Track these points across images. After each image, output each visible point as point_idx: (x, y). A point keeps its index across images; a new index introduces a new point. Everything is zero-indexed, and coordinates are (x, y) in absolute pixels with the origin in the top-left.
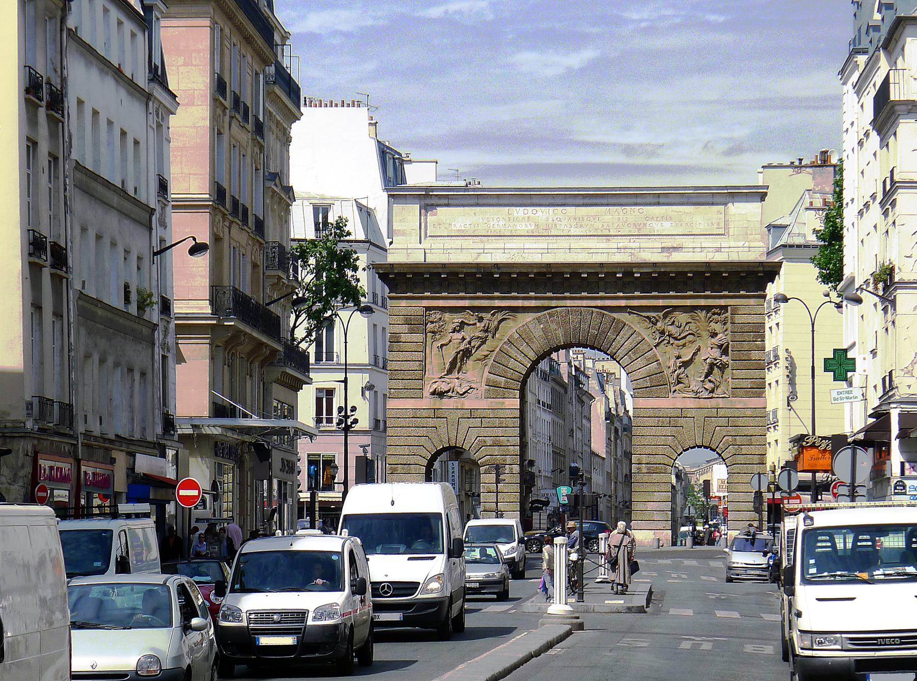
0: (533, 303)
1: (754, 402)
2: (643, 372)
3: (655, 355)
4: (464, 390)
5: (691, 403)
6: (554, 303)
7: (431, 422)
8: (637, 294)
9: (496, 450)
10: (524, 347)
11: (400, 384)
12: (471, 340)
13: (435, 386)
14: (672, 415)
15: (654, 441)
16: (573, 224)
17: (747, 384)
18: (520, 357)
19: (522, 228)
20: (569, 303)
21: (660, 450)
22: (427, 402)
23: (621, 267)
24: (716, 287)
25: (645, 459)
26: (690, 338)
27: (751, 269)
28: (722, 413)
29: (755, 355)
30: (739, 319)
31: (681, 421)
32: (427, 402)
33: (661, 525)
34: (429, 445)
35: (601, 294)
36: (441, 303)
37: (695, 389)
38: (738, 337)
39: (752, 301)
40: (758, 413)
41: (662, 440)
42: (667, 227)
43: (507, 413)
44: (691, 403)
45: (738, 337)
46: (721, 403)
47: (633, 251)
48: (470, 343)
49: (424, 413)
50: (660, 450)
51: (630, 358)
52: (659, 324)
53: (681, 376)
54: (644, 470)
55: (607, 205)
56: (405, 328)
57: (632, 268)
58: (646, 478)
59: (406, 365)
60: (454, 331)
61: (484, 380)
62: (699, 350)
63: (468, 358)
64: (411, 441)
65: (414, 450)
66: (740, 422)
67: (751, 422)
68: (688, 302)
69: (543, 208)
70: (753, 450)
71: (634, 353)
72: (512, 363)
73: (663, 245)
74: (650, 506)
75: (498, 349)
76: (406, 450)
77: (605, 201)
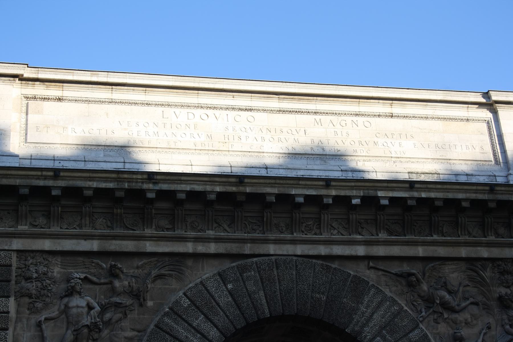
0: (213, 248)
8: (383, 236)
10: (199, 321)
12: (104, 309)
20: (272, 249)
24: (502, 230)
26: (475, 309)
35: (324, 236)
36: (47, 245)
52: (425, 287)
60: (71, 292)
68: (463, 252)
69: (217, 112)
73: (410, 170)
75: (152, 326)
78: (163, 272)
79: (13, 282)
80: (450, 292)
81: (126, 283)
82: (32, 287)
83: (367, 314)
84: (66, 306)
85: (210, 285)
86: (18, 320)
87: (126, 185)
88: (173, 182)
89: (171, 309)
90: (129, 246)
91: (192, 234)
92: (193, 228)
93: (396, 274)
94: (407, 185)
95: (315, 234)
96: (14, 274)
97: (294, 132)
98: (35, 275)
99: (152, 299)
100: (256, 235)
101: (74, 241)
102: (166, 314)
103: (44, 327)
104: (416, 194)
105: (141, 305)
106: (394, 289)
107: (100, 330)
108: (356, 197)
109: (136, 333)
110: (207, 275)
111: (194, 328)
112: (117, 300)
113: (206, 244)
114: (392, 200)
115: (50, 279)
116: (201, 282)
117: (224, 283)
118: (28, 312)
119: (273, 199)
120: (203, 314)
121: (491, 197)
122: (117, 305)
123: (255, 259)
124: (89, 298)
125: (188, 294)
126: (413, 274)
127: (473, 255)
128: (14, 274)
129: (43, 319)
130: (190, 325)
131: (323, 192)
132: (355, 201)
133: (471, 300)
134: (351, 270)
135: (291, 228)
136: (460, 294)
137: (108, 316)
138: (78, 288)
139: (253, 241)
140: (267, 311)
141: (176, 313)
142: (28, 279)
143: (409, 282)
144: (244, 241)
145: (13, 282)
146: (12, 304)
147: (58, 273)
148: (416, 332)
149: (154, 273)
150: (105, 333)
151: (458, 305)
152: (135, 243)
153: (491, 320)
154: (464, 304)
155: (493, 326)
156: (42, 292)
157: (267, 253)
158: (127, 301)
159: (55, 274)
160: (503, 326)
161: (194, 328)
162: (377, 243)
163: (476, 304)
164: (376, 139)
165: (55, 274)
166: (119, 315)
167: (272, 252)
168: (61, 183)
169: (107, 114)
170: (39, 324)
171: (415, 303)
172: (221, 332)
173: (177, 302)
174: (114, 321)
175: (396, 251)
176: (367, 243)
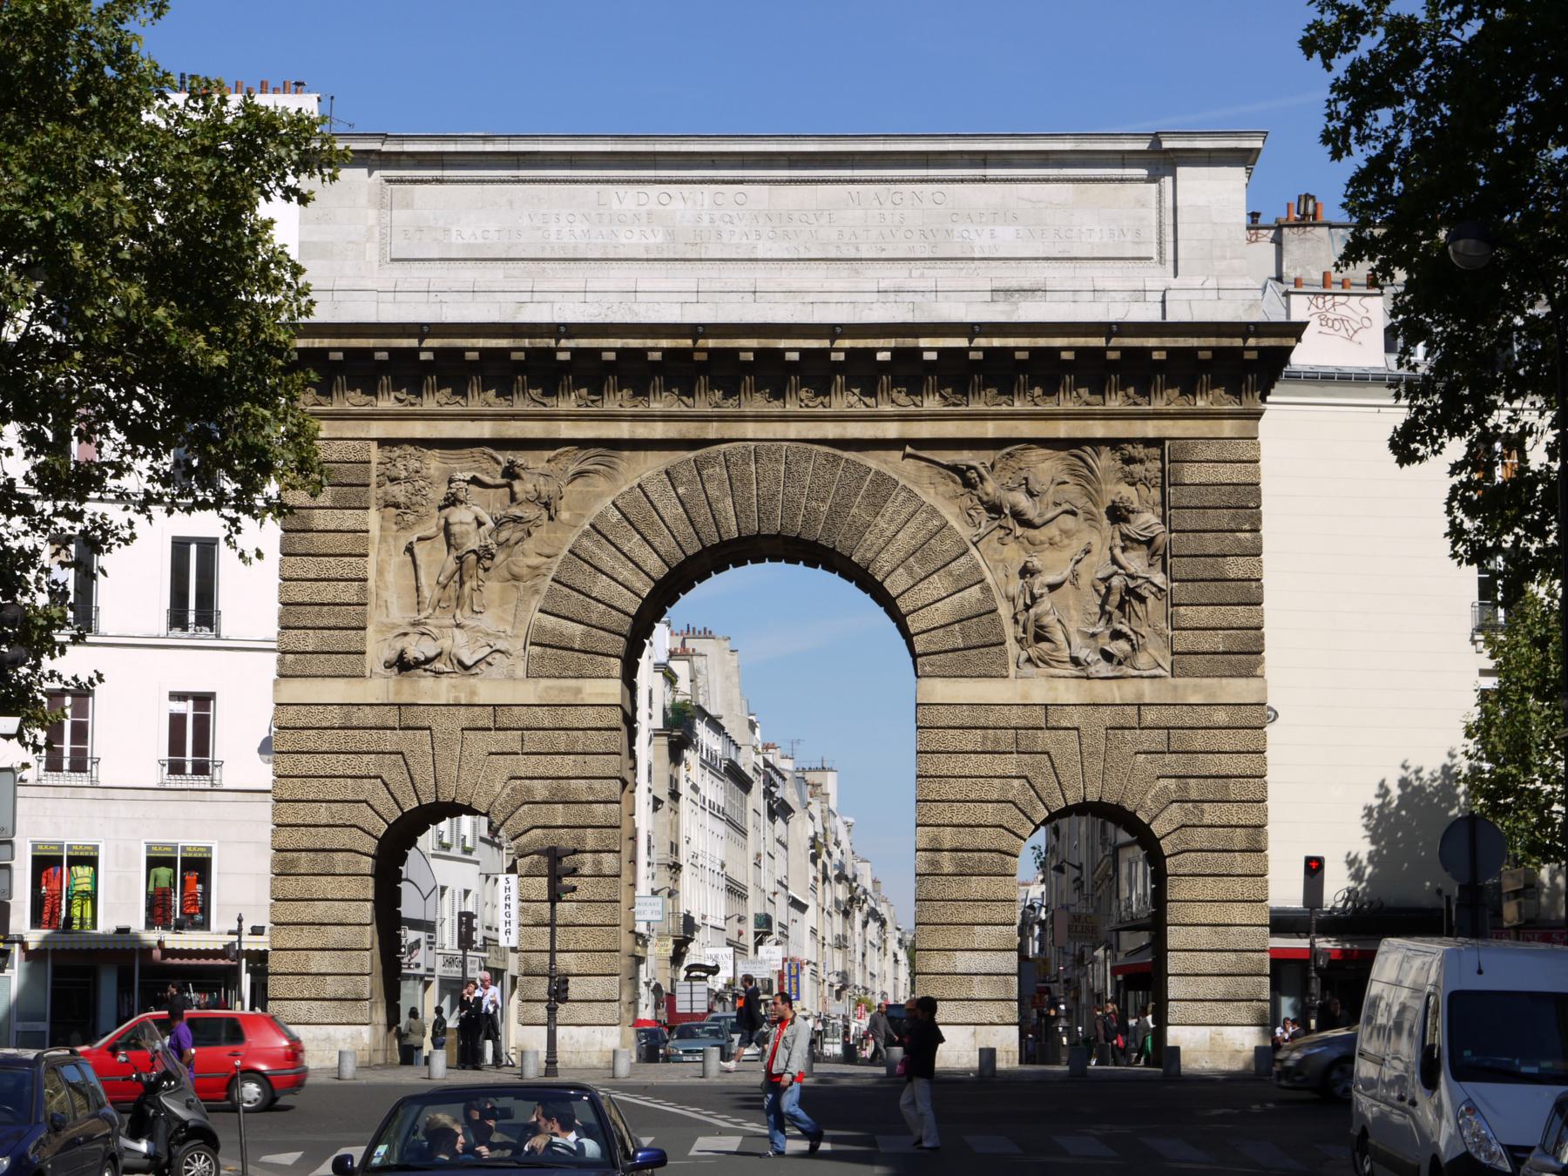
0: (659, 431)
1: (1236, 689)
2: (943, 611)
3: (977, 567)
5: (1067, 691)
6: (712, 431)
7: (391, 740)
8: (932, 403)
9: (559, 814)
10: (633, 544)
11: (311, 641)
12: (499, 524)
14: (1021, 723)
15: (976, 790)
17: (1217, 641)
18: (626, 572)
19: (631, 240)
20: (750, 430)
25: (948, 837)
26: (1068, 522)
28: (1150, 716)
29: (1235, 567)
30: (1192, 474)
31: (1045, 739)
32: (378, 687)
33: (992, 1011)
34: (382, 799)
36: (418, 430)
37: (1082, 654)
38: (1190, 520)
39: (1228, 428)
40: (1245, 716)
41: (995, 789)
42: (1007, 239)
43: (590, 718)
44: (1067, 691)
45: (1190, 520)
46: (1148, 690)
47: (918, 298)
49: (370, 717)
50: (989, 813)
51: (910, 570)
52: (991, 487)
53: (1047, 620)
54: (948, 867)
55: (852, 181)
58: (955, 888)
59: (328, 592)
60: (452, 501)
62: (1087, 552)
64: (334, 789)
65: (346, 813)
66: (1199, 740)
67: (1226, 740)
68: (1063, 430)
70: (1235, 814)
71: (923, 561)
72: (601, 586)
73: (997, 285)
74: (963, 962)
75: (566, 552)
76: (323, 814)
78: (585, 466)
79: (373, 486)
80: (1031, 494)
81: (530, 487)
82: (399, 492)
83: (888, 533)
85: (649, 489)
86: (383, 539)
87: (526, 343)
89: (592, 526)
90: (535, 430)
93: (947, 467)
96: (374, 474)
97: (812, 219)
98: (403, 474)
99: (569, 509)
102: (586, 534)
103: (416, 550)
105: (551, 518)
106: (941, 489)
107: (493, 557)
109: (544, 559)
110: (649, 473)
112: (516, 511)
115: (424, 478)
116: (639, 486)
118: (395, 527)
119: (750, 356)
122: (517, 520)
123: (724, 446)
124: (477, 509)
125: (619, 503)
126: (974, 468)
127: (1079, 434)
128: (374, 474)
132: (883, 356)
133: (1066, 507)
134: (872, 460)
136: (1049, 498)
137: (504, 535)
138: (461, 495)
139: (722, 418)
140: (734, 528)
141: (599, 532)
142: (393, 480)
143: (966, 478)
145: (373, 486)
146: (373, 519)
147: (438, 469)
148: (962, 560)
149: (573, 468)
150: (499, 558)
151: (1040, 515)
153: (1095, 539)
154: (1049, 515)
155: (1095, 550)
156: (414, 499)
158: (530, 512)
159: (432, 471)
160: (1111, 549)
163: (1074, 513)
164: (950, 226)
165: (432, 471)
166: (518, 535)
167: (750, 436)
169: (511, 203)
170: (410, 550)
171: (972, 512)
173: (601, 515)
174: (512, 542)
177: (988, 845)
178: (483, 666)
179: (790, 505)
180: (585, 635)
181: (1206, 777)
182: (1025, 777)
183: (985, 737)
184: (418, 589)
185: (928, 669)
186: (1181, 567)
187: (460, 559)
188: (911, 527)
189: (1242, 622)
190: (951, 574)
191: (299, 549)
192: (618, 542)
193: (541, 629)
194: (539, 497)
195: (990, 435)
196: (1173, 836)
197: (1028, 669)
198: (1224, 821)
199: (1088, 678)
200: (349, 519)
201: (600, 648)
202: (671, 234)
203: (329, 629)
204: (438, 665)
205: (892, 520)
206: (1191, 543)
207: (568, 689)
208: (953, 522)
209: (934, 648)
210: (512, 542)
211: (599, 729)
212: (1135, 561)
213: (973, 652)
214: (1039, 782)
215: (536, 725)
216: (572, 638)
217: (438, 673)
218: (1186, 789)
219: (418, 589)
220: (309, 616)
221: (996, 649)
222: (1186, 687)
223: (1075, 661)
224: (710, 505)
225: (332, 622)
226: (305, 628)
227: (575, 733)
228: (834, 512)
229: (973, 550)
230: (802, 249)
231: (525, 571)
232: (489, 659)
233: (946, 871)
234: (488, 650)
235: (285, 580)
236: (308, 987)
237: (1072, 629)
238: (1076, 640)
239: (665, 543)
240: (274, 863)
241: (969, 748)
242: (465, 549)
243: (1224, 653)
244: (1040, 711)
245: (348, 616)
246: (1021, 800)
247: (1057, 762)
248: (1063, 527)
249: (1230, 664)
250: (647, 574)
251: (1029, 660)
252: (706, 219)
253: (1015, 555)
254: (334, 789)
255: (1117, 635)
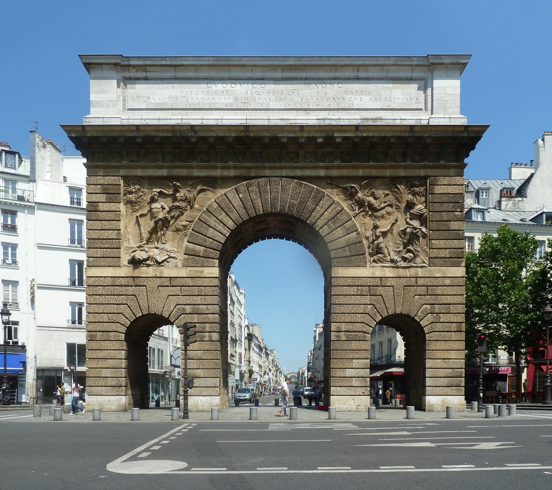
0: (232, 173)
2: (342, 241)
3: (355, 225)
4: (163, 259)
5: (389, 273)
8: (337, 163)
10: (223, 216)
13: (133, 254)
16: (273, 98)
18: (220, 227)
21: (359, 318)
22: (125, 271)
23: (322, 131)
27: (455, 135)
28: (420, 281)
31: (380, 290)
37: (396, 258)
38: (437, 207)
41: (361, 309)
43: (206, 282)
44: (389, 273)
45: (437, 207)
46: (420, 272)
48: (169, 212)
51: (329, 227)
56: (103, 198)
57: (333, 132)
59: (105, 234)
61: (183, 249)
63: (167, 228)
66: (439, 291)
71: (334, 223)
72: (211, 232)
75: (197, 219)
77: (304, 75)
83: (321, 212)
84: (151, 209)
88: (206, 131)
91: (219, 164)
92: (222, 161)
94: (354, 128)
95: (295, 162)
97: (291, 93)
99: (198, 204)
100: (258, 164)
101: (154, 170)
102: (204, 212)
104: (360, 134)
108: (320, 137)
111: (219, 220)
112: (177, 204)
113: (229, 170)
114: (345, 138)
117: (238, 194)
120: (225, 212)
121: (411, 134)
122: (178, 207)
129: (138, 214)
130: (217, 218)
131: (299, 135)
135: (280, 159)
138: (156, 197)
139: (256, 168)
141: (210, 212)
144: (250, 168)
145: (122, 194)
146: (122, 207)
152: (188, 170)
157: (264, 175)
161: (219, 220)
162: (333, 167)
168: (141, 134)
172: (234, 223)
175: (345, 172)
176: (327, 168)
177: (359, 330)
178: (165, 263)
179: (283, 201)
180: (205, 251)
181: (441, 304)
182: (373, 304)
183: (358, 290)
184: (140, 234)
185: (336, 263)
186: (434, 225)
187: (156, 223)
188: (330, 210)
189: (457, 246)
190: (345, 228)
191: (93, 218)
192: (217, 216)
193: (187, 248)
194: (186, 199)
195: (360, 175)
196: (429, 326)
197: (374, 264)
198: (448, 321)
199: (398, 267)
200: (113, 206)
201: (211, 255)
202: (236, 99)
203: (106, 248)
204: (148, 262)
205: (322, 207)
206: (437, 216)
207: (198, 271)
208: (345, 208)
209: (338, 256)
210: (176, 216)
211: (210, 286)
212: (416, 223)
213: (354, 257)
214: (378, 306)
215: (186, 285)
216: (200, 252)
217: (149, 266)
218: (434, 308)
219: (140, 234)
220: (98, 244)
221: (362, 256)
222: (434, 270)
223: (392, 261)
224: (252, 201)
225: (107, 246)
226: (97, 248)
227: (201, 288)
228: (301, 203)
229: (353, 219)
230: (287, 105)
231: (181, 227)
232: (168, 260)
233: (342, 339)
234: (167, 257)
235: (88, 230)
236: (101, 382)
237: (390, 249)
238: (392, 253)
239: (234, 215)
240: (87, 336)
241: (352, 293)
242: (158, 218)
243: (449, 258)
244: (379, 280)
245: (114, 243)
246: (371, 313)
247: (385, 298)
248: (388, 211)
249: (451, 262)
250: (228, 228)
251: (374, 261)
252: (249, 93)
253: (368, 220)
254: (109, 309)
255: (409, 251)
